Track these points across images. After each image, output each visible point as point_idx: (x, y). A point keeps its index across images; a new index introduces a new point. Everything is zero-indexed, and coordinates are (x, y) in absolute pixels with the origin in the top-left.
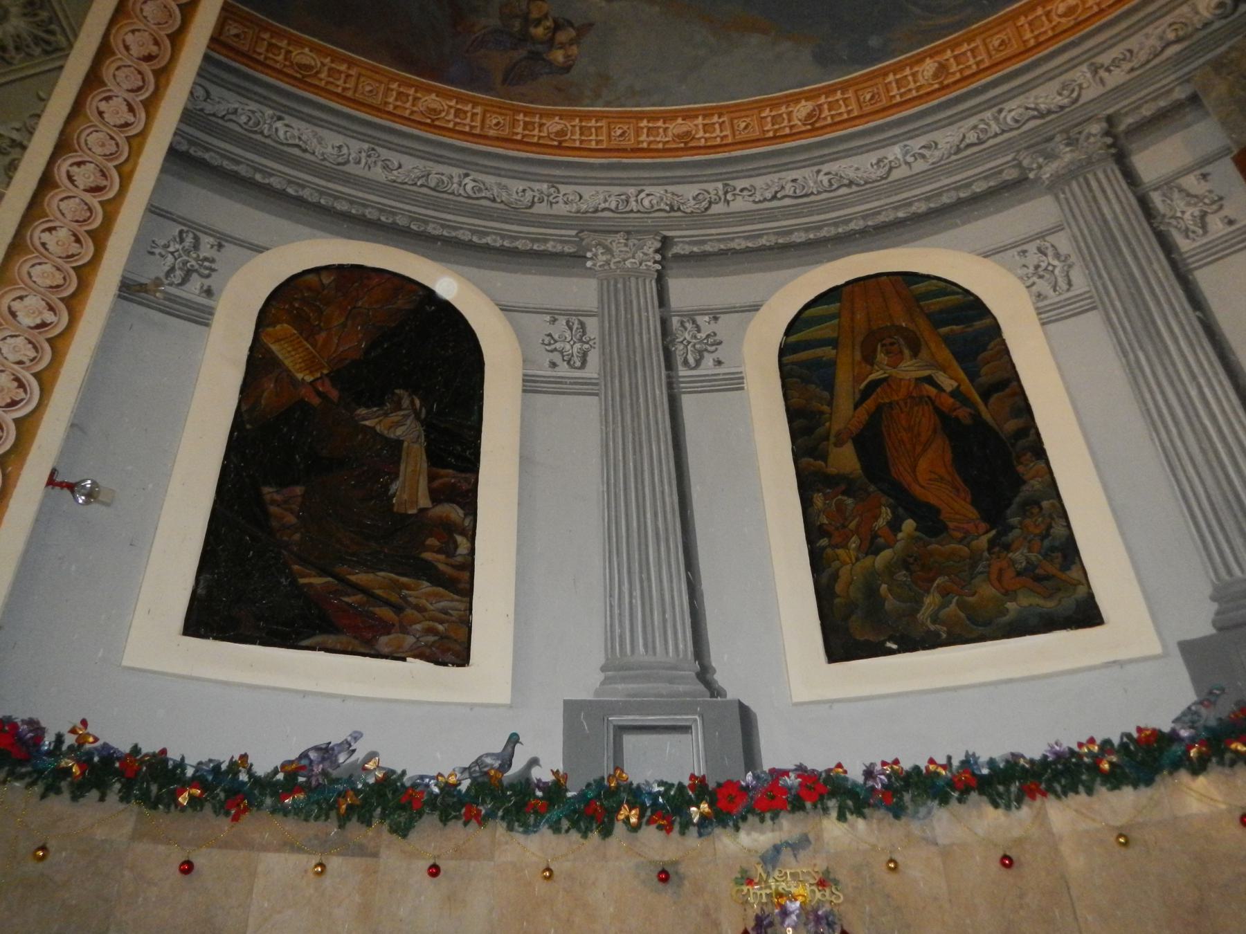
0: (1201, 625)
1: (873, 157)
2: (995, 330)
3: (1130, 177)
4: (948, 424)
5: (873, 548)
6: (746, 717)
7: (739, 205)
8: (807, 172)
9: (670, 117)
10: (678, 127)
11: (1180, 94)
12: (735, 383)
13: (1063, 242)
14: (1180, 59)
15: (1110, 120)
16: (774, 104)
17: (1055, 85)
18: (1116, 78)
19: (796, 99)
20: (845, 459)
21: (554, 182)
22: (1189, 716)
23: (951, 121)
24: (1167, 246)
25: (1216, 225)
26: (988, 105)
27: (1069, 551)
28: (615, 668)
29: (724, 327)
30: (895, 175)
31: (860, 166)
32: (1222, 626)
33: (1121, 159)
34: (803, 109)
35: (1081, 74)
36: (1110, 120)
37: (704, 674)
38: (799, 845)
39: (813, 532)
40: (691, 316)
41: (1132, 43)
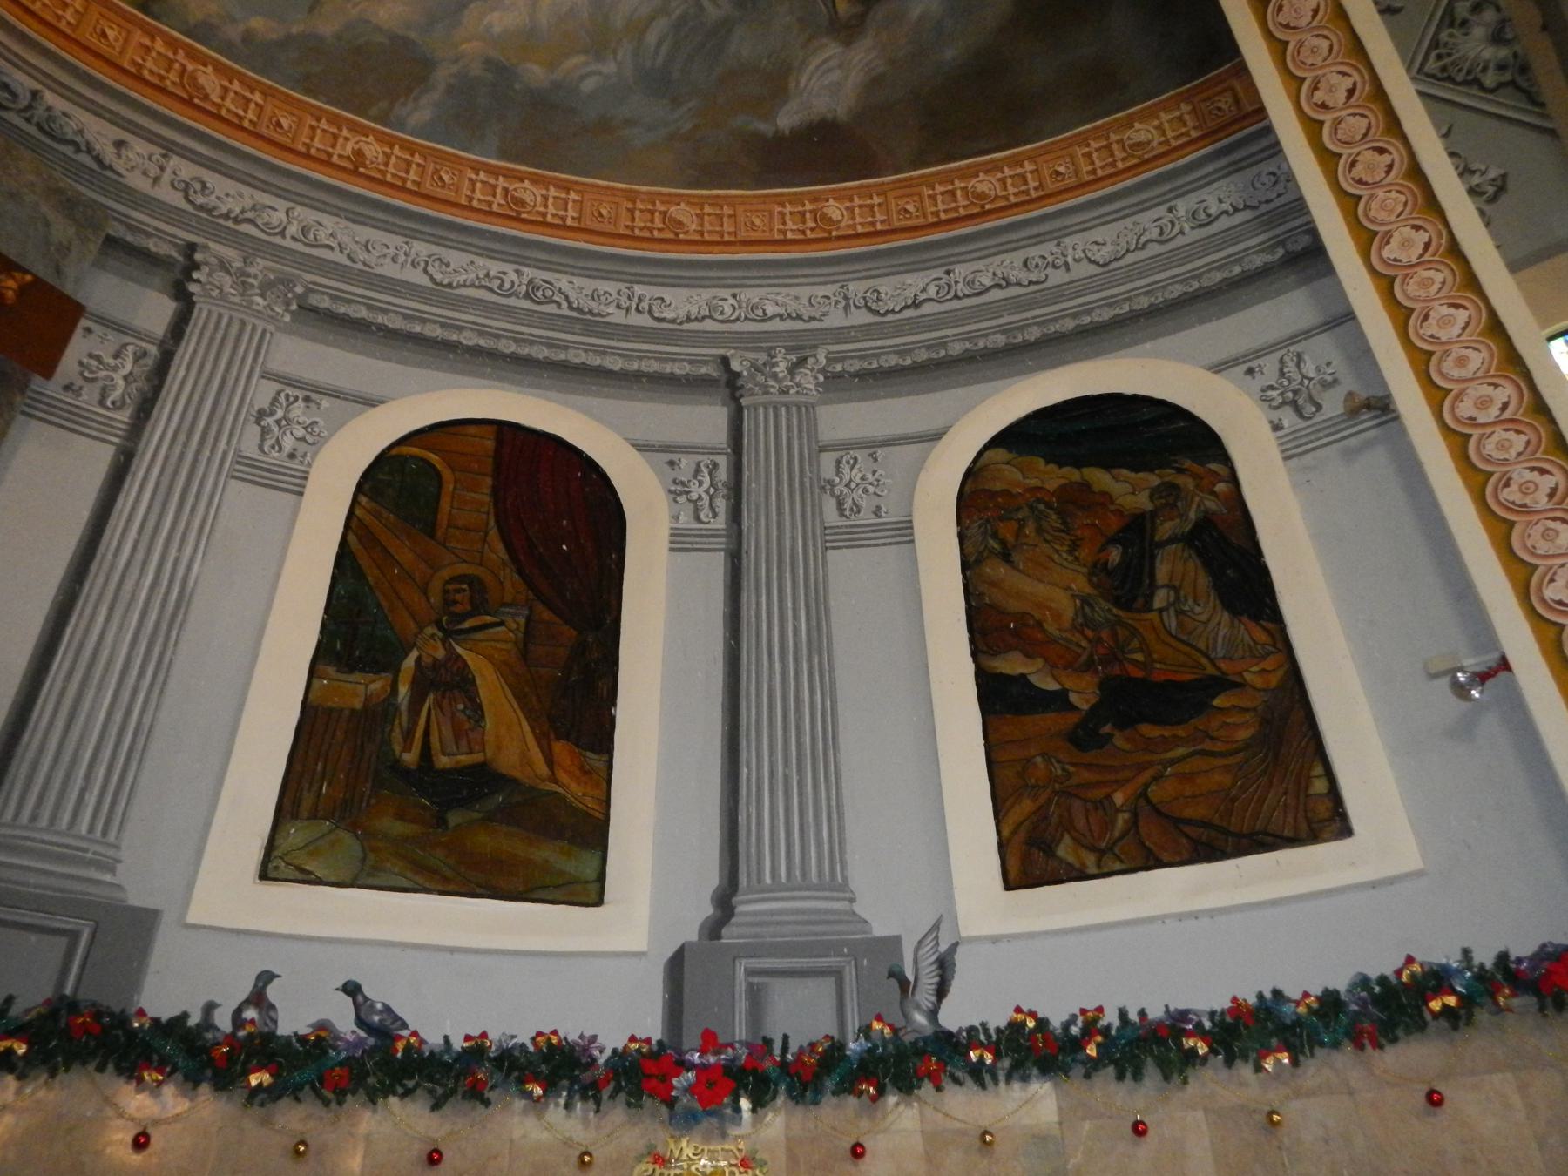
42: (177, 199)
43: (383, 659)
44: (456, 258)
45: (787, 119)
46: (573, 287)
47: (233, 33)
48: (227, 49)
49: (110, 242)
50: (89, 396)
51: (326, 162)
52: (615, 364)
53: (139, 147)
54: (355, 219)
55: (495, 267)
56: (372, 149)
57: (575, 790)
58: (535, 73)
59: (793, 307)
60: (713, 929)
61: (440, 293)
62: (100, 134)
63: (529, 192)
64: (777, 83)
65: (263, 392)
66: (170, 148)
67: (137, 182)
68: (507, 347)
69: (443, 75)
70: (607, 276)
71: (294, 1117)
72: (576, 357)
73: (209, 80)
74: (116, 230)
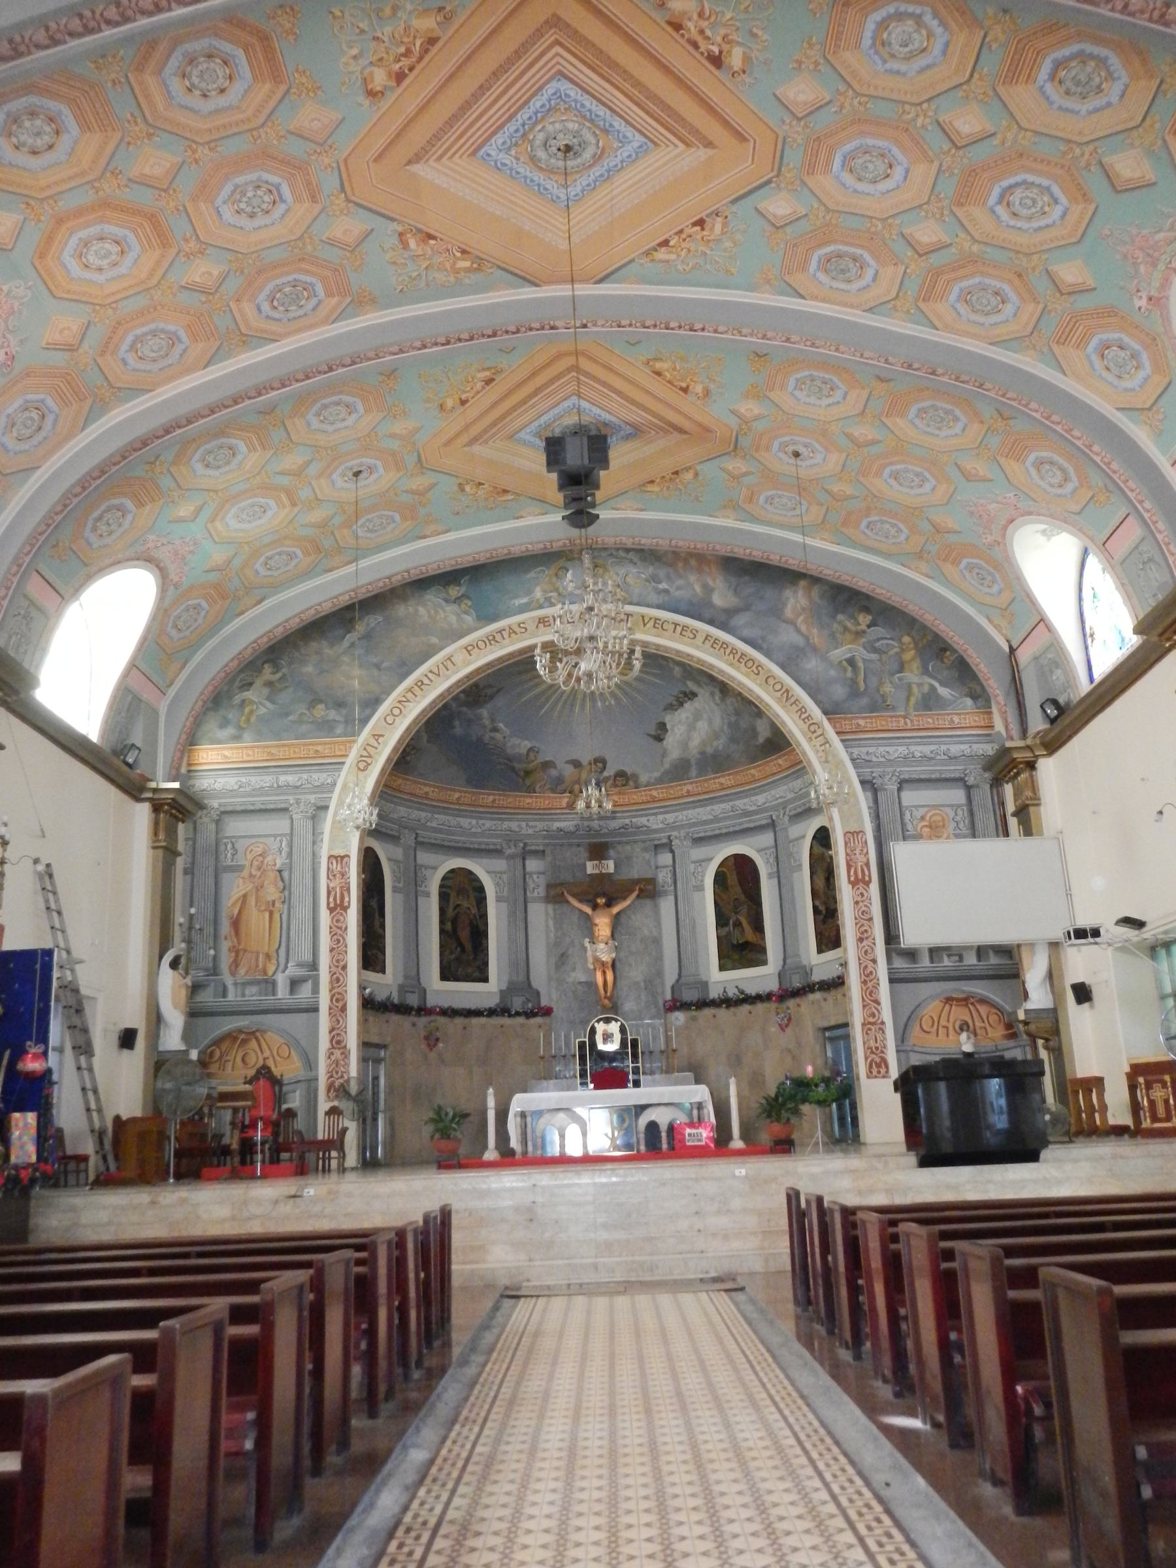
0: (504, 987)
1: (469, 820)
2: (485, 898)
3: (524, 865)
4: (471, 923)
5: (452, 953)
6: (425, 991)
7: (434, 824)
8: (450, 818)
9: (425, 785)
10: (426, 789)
11: (541, 848)
12: (428, 895)
13: (505, 877)
14: (545, 837)
15: (525, 844)
16: (451, 790)
17: (516, 823)
18: (530, 831)
19: (454, 790)
20: (449, 926)
21: (395, 804)
22: (497, 1005)
23: (492, 819)
24: (525, 894)
25: (536, 894)
26: (500, 819)
27: (486, 964)
28: (406, 977)
29: (428, 873)
30: (473, 830)
31: (465, 822)
32: (508, 988)
33: (524, 859)
34: (457, 795)
35: (523, 824)
36: (525, 844)
37: (419, 980)
38: (434, 1021)
39: (441, 946)
40: (422, 866)
41: (537, 823)
42: (661, 826)
43: (726, 924)
44: (715, 807)
45: (761, 740)
46: (740, 804)
47: (653, 780)
48: (654, 784)
49: (656, 847)
50: (666, 887)
51: (683, 797)
52: (752, 825)
53: (651, 818)
54: (694, 808)
55: (723, 806)
56: (690, 787)
57: (760, 942)
58: (709, 750)
59: (782, 794)
60: (783, 966)
61: (716, 819)
62: (643, 820)
63: (722, 780)
64: (754, 733)
65: (692, 866)
66: (655, 814)
67: (655, 827)
68: (731, 829)
69: (693, 761)
70: (746, 797)
71: (732, 1009)
72: (746, 826)
73: (654, 793)
74: (656, 842)
